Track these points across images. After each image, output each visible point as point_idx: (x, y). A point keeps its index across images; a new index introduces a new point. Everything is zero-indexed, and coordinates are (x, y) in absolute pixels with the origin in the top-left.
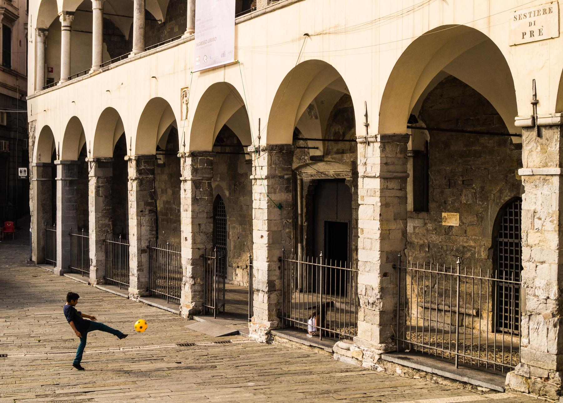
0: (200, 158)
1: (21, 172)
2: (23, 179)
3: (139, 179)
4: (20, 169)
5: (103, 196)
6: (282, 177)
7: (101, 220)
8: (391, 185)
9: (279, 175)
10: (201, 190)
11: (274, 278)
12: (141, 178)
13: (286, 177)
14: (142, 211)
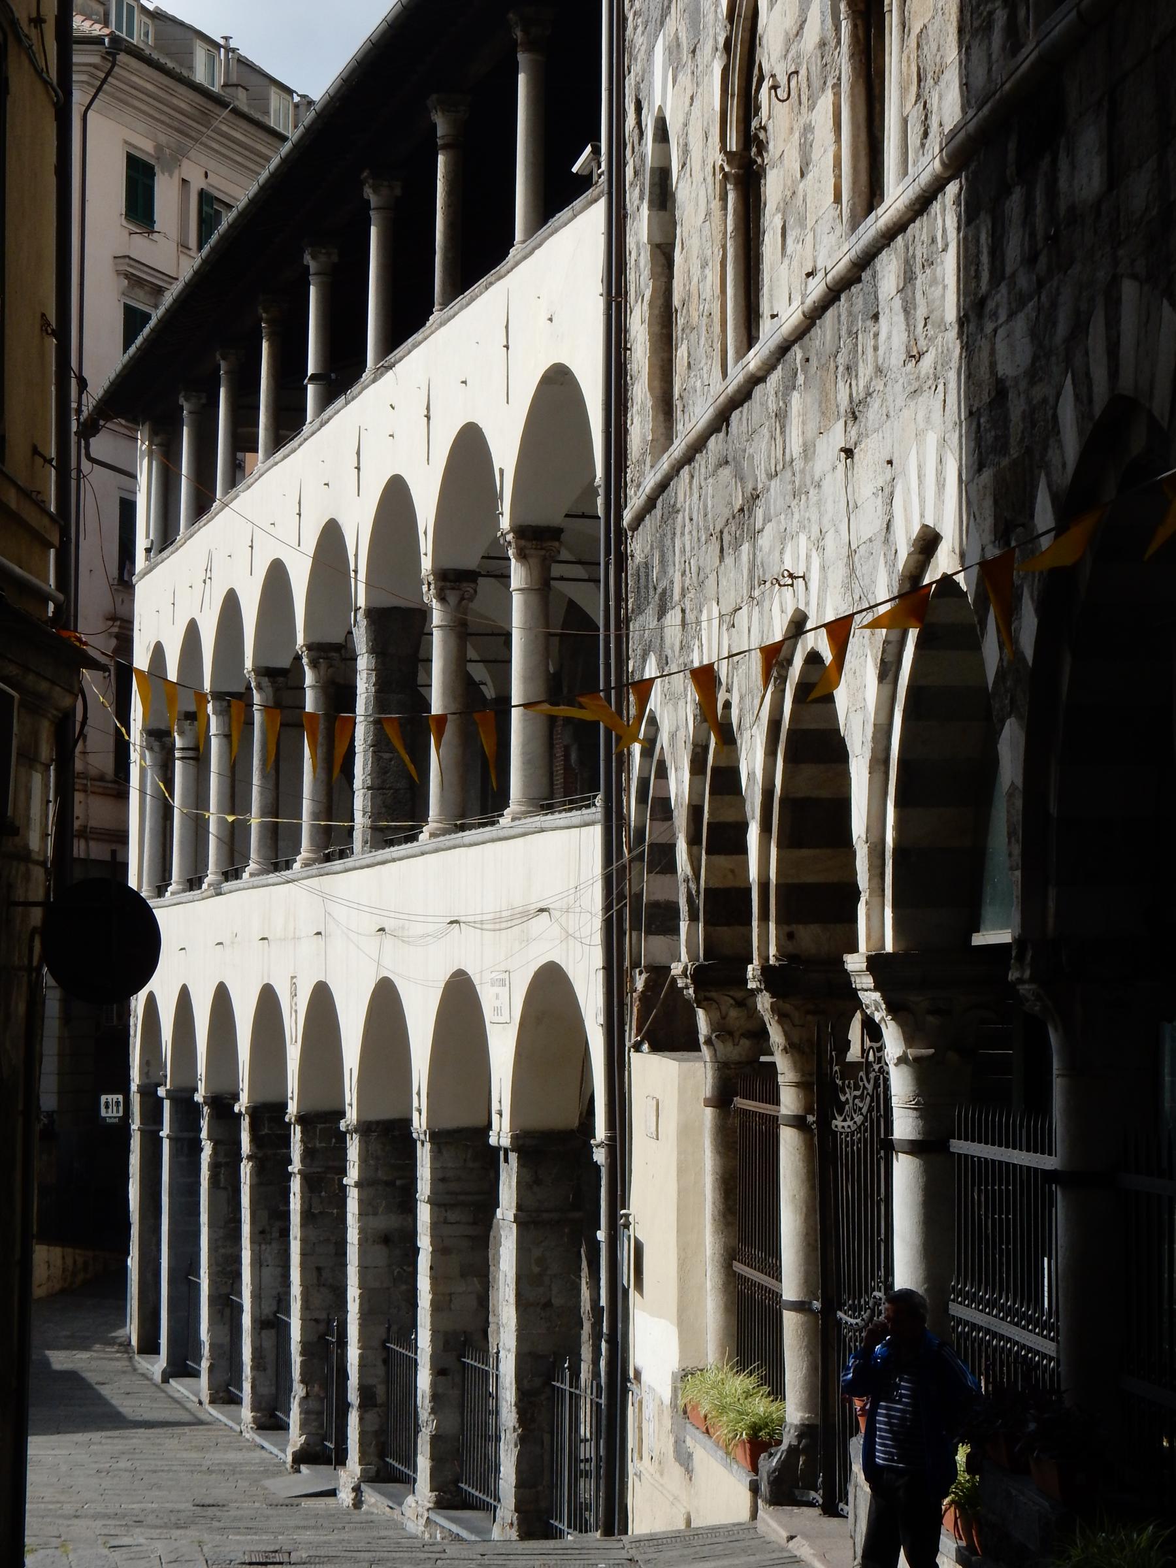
0: (319, 1126)
1: (107, 1107)
2: (112, 1125)
3: (256, 1158)
4: (103, 1098)
5: (230, 1188)
6: (389, 1184)
7: (224, 1247)
8: (452, 1216)
9: (385, 1178)
10: (323, 1194)
11: (371, 1381)
12: (260, 1155)
13: (398, 1183)
14: (262, 1232)
